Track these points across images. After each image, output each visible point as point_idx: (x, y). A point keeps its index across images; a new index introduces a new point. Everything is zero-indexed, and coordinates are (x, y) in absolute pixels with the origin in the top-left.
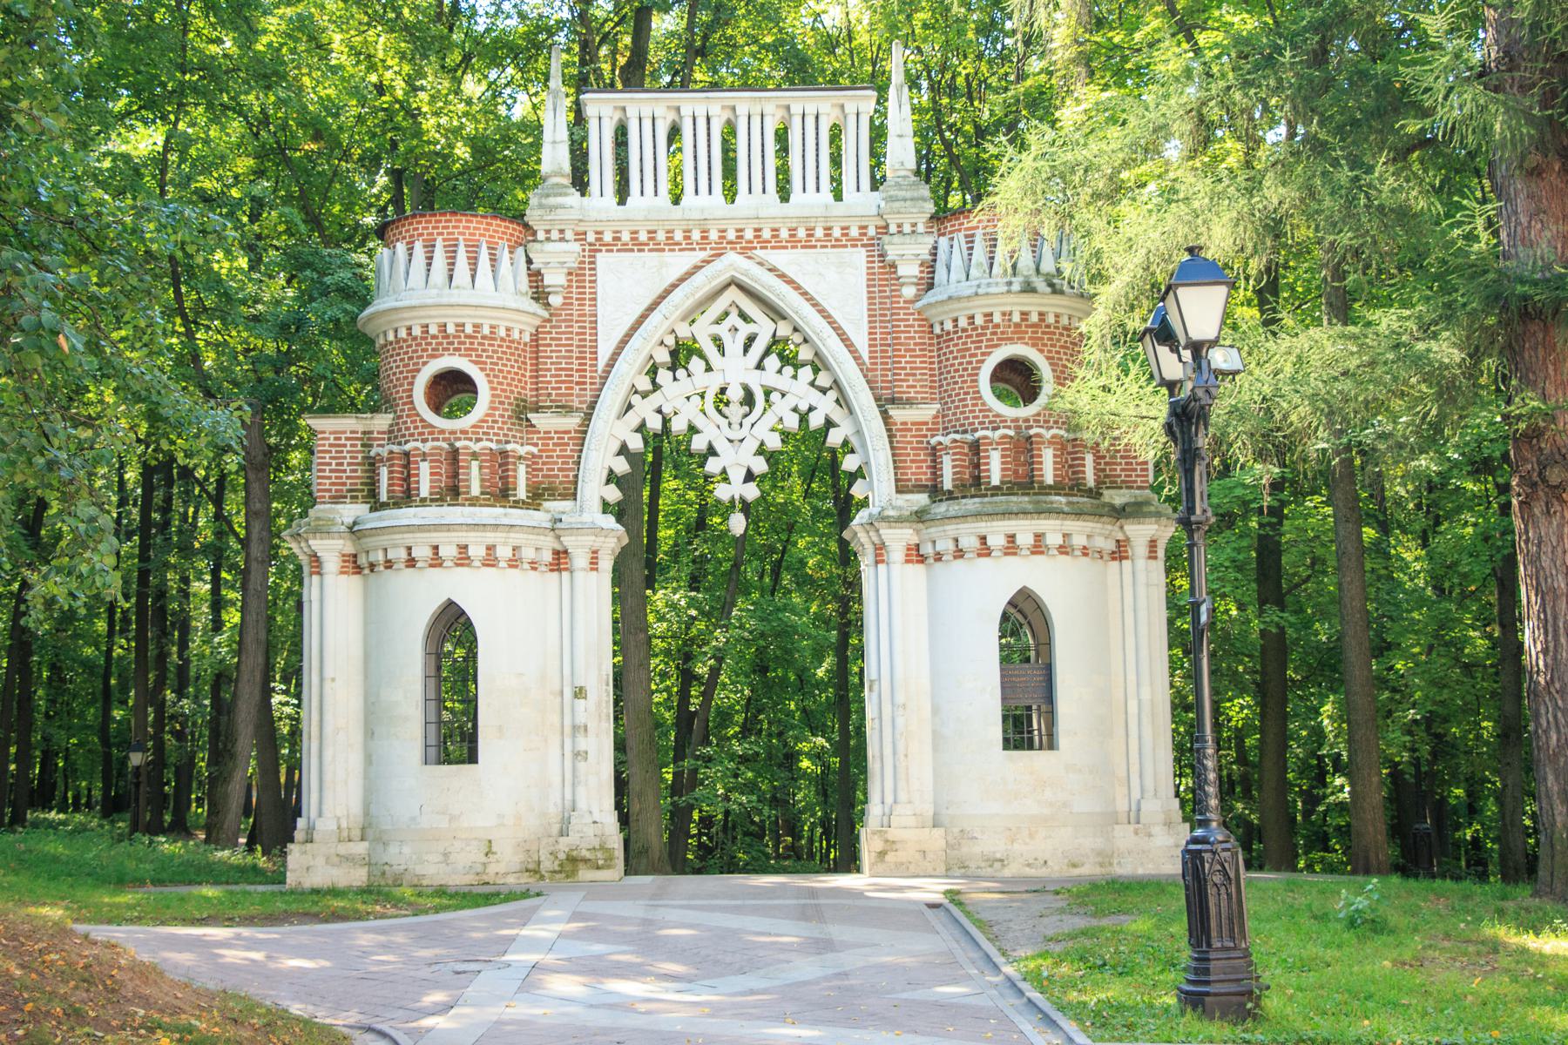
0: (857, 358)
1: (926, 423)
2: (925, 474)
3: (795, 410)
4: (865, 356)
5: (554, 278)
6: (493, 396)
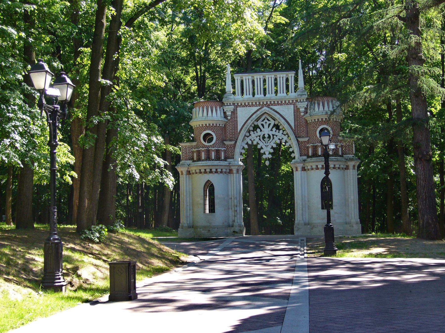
3: (279, 139)
5: (229, 113)
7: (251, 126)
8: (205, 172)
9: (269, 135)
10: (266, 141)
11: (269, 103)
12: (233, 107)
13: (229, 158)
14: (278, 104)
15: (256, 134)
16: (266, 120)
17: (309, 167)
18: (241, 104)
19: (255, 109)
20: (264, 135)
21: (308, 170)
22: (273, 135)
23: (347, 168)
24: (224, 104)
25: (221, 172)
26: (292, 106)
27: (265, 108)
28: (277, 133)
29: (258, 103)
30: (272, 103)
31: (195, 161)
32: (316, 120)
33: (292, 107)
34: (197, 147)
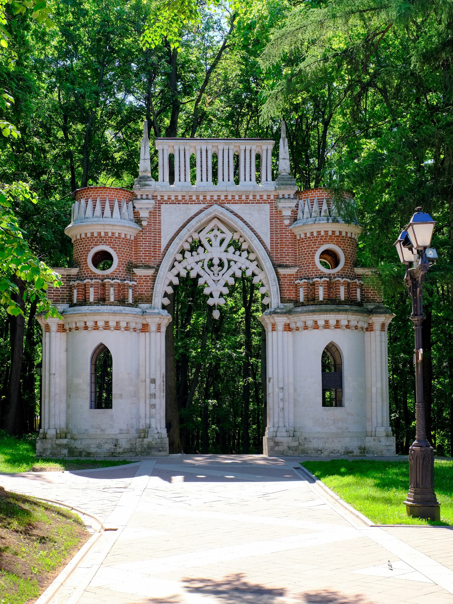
0: (266, 248)
1: (293, 275)
2: (292, 295)
3: (240, 269)
4: (269, 247)
5: (144, 214)
6: (119, 261)
7: (187, 241)
8: (96, 328)
9: (220, 260)
10: (216, 272)
11: (223, 198)
12: (153, 201)
13: (143, 302)
14: (240, 201)
15: (197, 258)
16: (216, 232)
17: (300, 324)
18: (169, 199)
19: (195, 208)
20: (211, 260)
21: (298, 330)
23: (370, 328)
24: (136, 196)
25: (127, 329)
26: (267, 206)
27: (216, 207)
29: (201, 198)
30: (230, 198)
31: (75, 305)
33: (267, 206)
34: (78, 277)
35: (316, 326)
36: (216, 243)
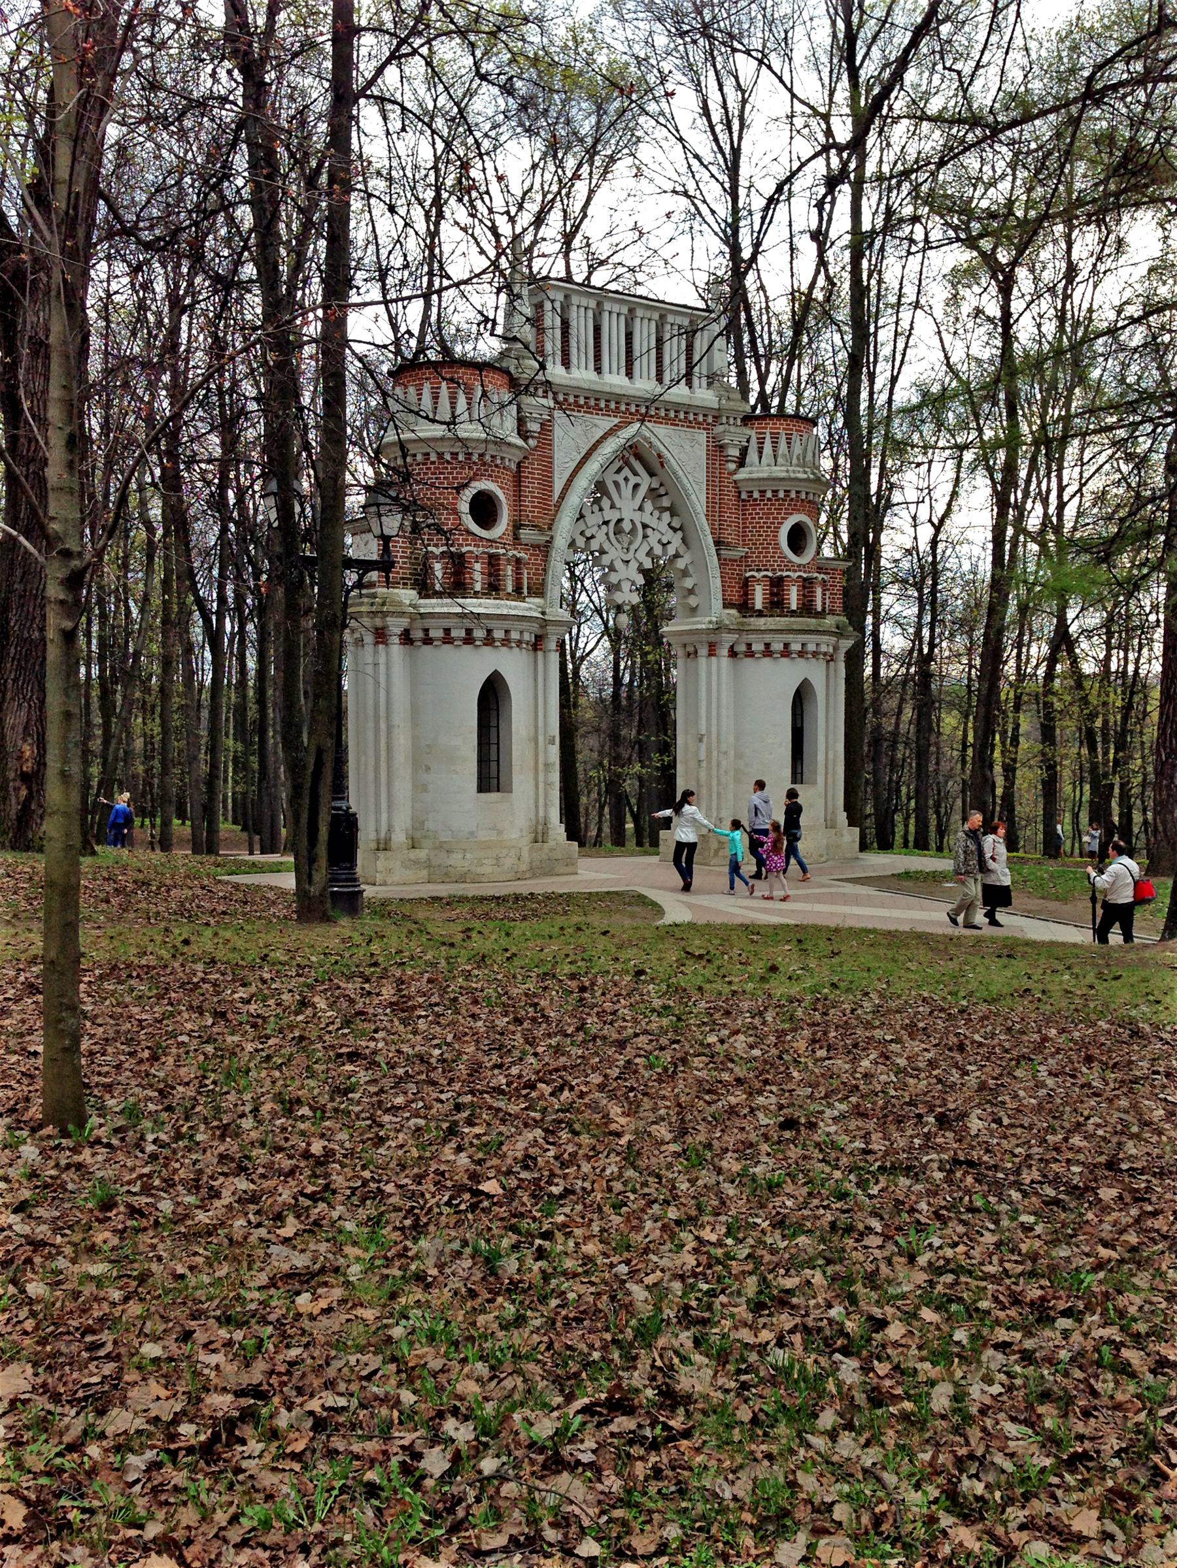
8: (489, 641)
16: (626, 472)
22: (645, 526)
28: (652, 522)
32: (781, 495)
33: (702, 437)
35: (786, 652)
36: (627, 491)
